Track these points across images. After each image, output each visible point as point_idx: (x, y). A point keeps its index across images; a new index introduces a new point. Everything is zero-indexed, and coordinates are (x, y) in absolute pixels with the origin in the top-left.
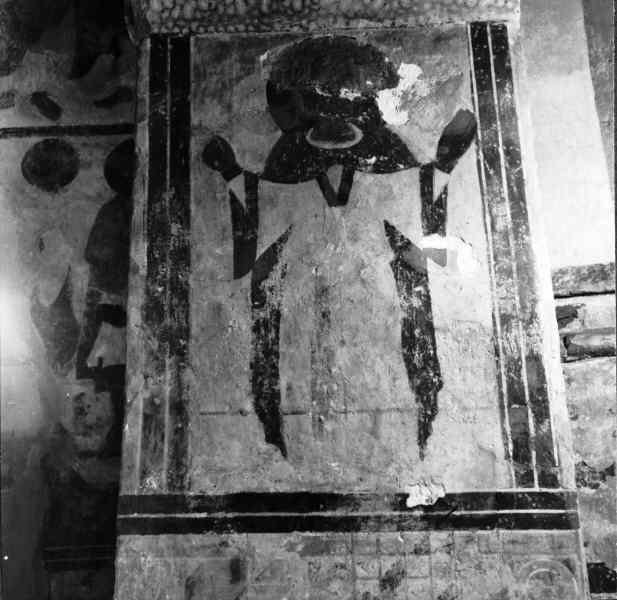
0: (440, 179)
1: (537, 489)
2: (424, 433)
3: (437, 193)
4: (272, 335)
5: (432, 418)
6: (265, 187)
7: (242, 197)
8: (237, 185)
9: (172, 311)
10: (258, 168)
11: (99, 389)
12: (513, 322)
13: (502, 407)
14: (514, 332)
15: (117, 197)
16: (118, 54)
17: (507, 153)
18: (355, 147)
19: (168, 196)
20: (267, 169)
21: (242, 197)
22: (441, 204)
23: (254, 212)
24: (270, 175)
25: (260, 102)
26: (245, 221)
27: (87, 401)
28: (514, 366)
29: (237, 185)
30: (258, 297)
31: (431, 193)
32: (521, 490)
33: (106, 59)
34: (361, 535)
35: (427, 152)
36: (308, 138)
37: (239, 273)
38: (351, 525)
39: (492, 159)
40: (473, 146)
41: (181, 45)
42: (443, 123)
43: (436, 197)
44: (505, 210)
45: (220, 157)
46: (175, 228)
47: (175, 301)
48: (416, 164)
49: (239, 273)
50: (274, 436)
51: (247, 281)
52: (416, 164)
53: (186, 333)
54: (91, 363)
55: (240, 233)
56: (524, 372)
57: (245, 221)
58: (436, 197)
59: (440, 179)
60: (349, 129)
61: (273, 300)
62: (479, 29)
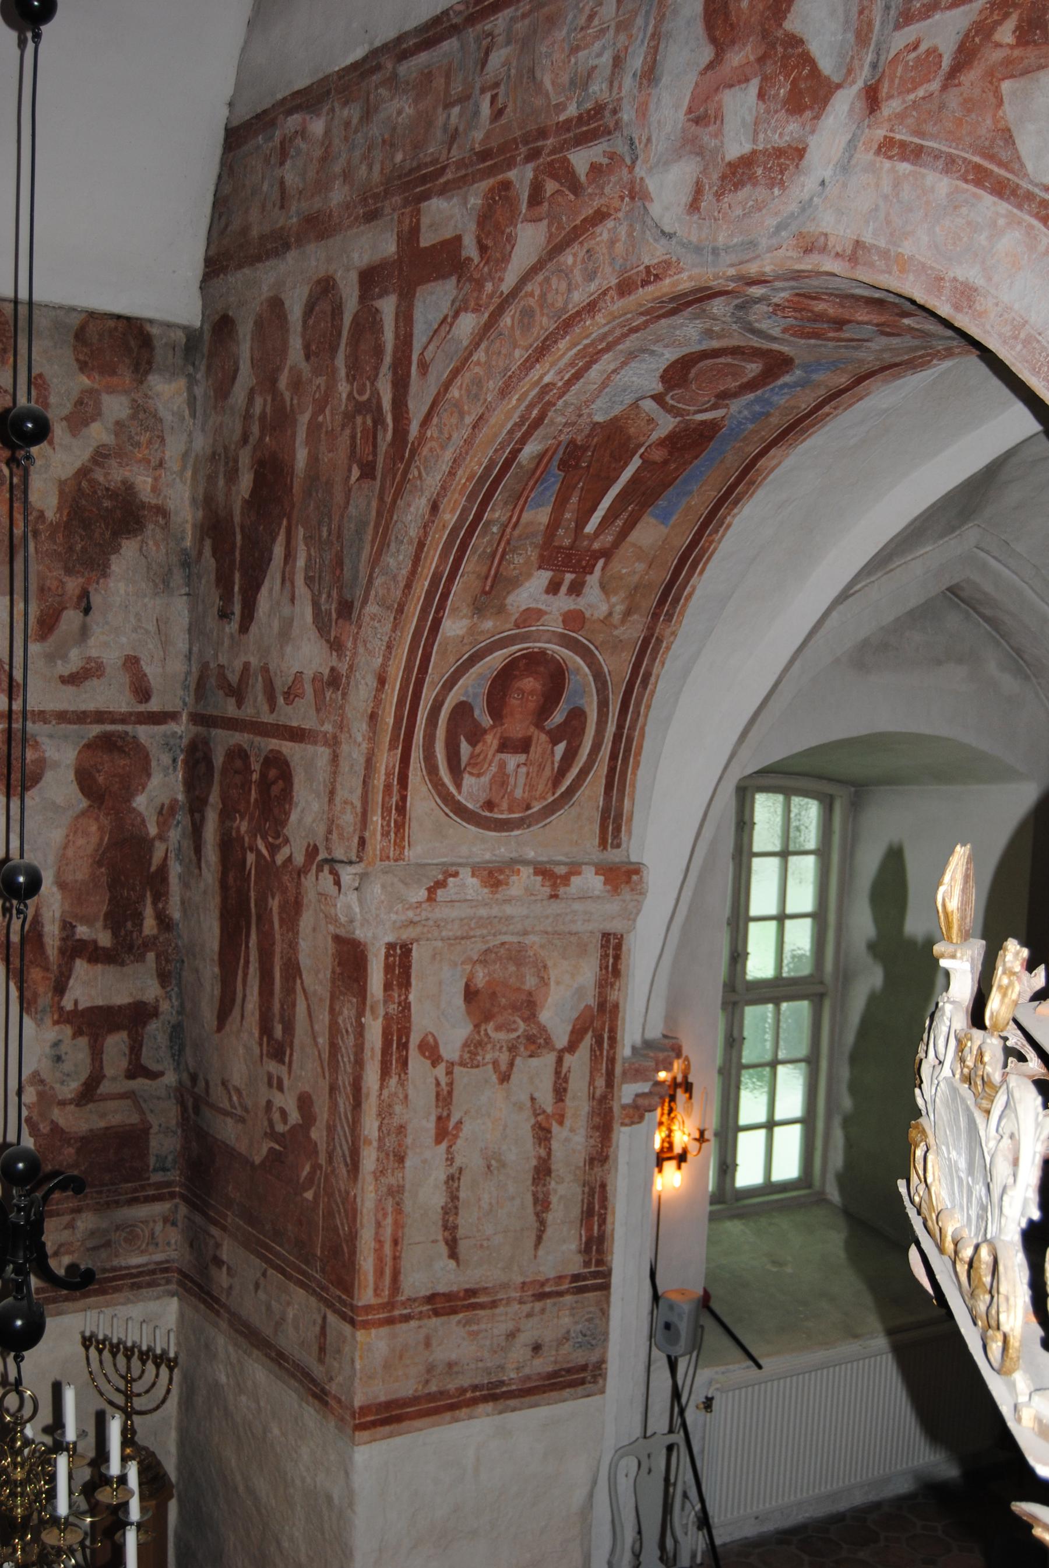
0: (568, 1058)
1: (593, 1269)
2: (539, 1239)
3: (564, 1070)
4: (456, 1185)
5: (543, 1231)
6: (457, 1069)
7: (443, 1081)
8: (440, 1070)
9: (393, 1172)
10: (455, 1056)
11: (78, 1033)
12: (596, 1163)
13: (582, 1220)
14: (596, 1169)
15: (90, 806)
16: (87, 610)
17: (610, 1038)
18: (518, 1037)
19: (393, 1081)
20: (461, 1057)
21: (443, 1081)
22: (566, 1080)
23: (450, 1093)
24: (462, 1064)
25: (459, 1001)
26: (444, 1098)
27: (64, 1048)
28: (592, 1193)
29: (440, 1070)
30: (450, 1160)
31: (560, 1072)
32: (586, 1270)
33: (71, 618)
34: (497, 1311)
35: (561, 1040)
36: (489, 1032)
37: (438, 1140)
38: (494, 1304)
39: (599, 1041)
40: (590, 1034)
41: (406, 950)
42: (575, 1015)
43: (563, 1075)
44: (601, 1082)
45: (431, 1051)
46: (398, 1109)
47: (396, 1165)
48: (553, 1049)
49: (438, 1140)
50: (453, 1255)
51: (444, 1145)
52: (553, 1049)
53: (401, 1189)
54: (68, 1004)
55: (440, 1110)
56: (596, 1196)
57: (444, 1098)
58: (563, 1075)
59: (568, 1058)
60: (514, 1022)
61: (458, 1163)
62: (606, 936)
